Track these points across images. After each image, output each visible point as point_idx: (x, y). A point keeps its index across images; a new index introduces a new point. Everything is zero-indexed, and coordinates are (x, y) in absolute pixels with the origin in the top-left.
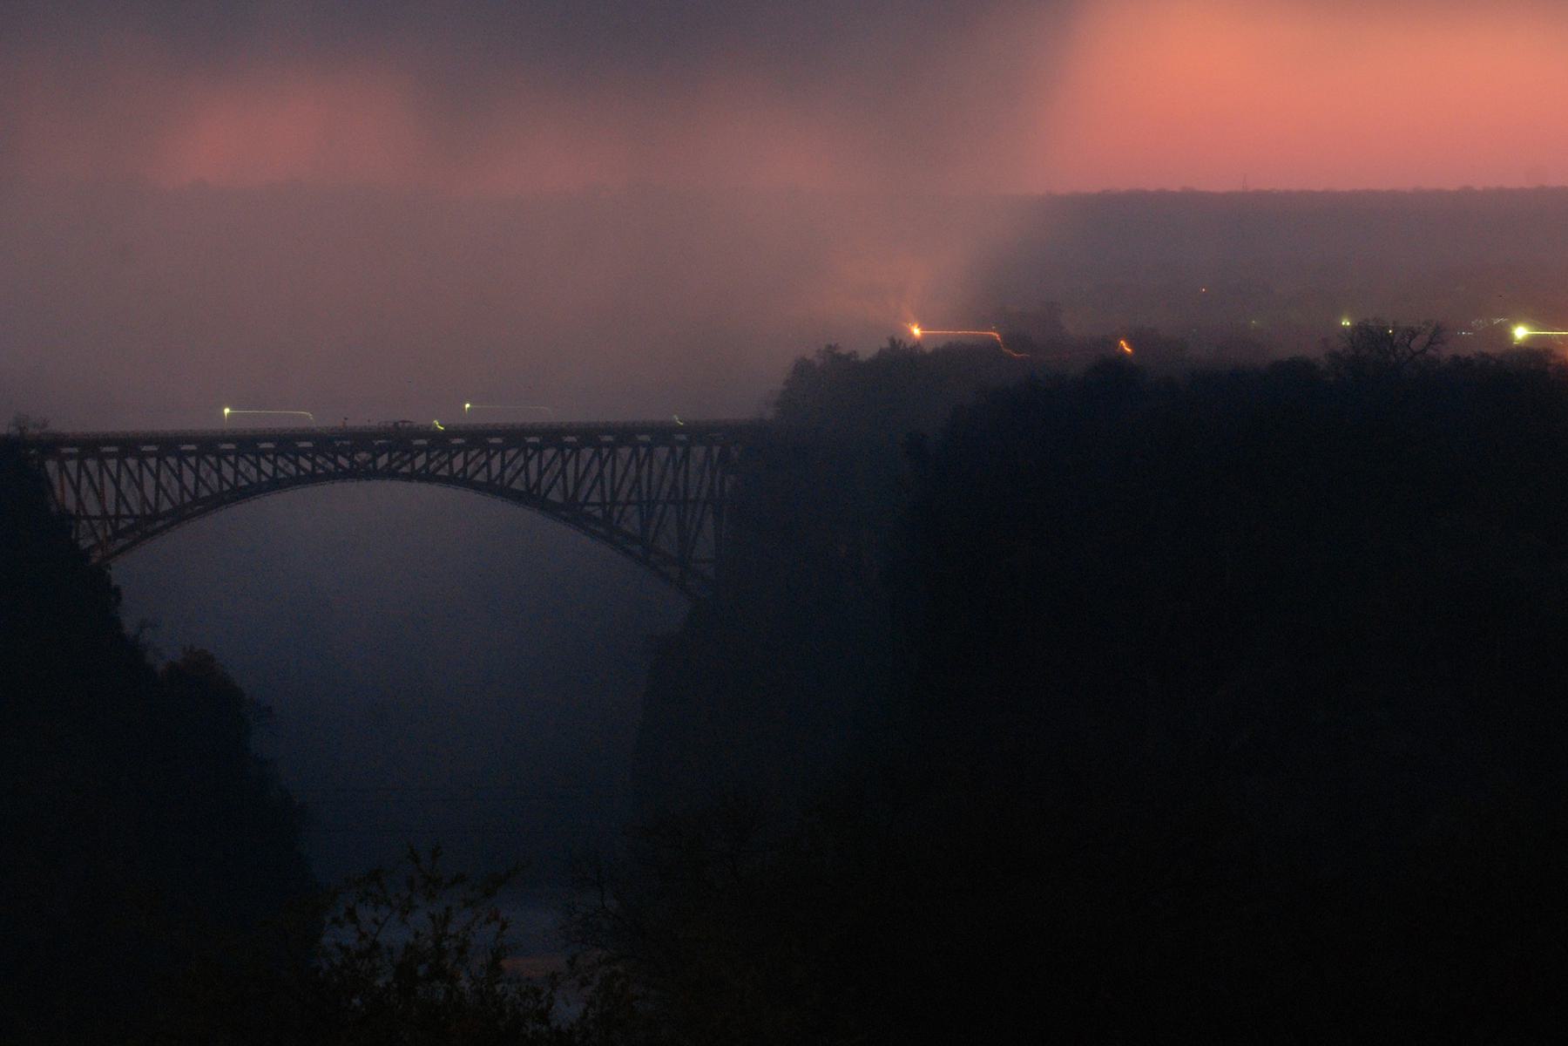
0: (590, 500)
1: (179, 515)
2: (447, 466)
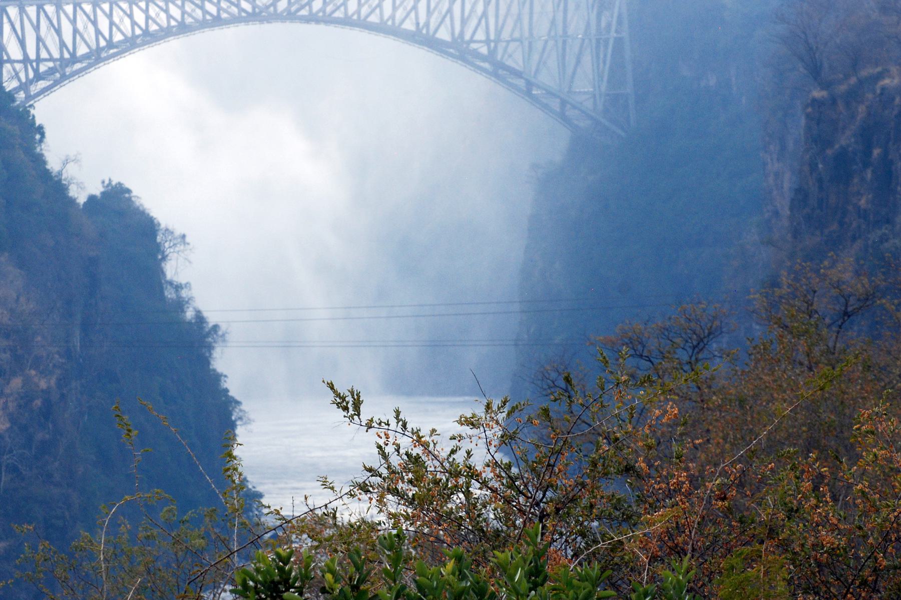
0: (477, 37)
1: (96, 57)
2: (342, 9)
